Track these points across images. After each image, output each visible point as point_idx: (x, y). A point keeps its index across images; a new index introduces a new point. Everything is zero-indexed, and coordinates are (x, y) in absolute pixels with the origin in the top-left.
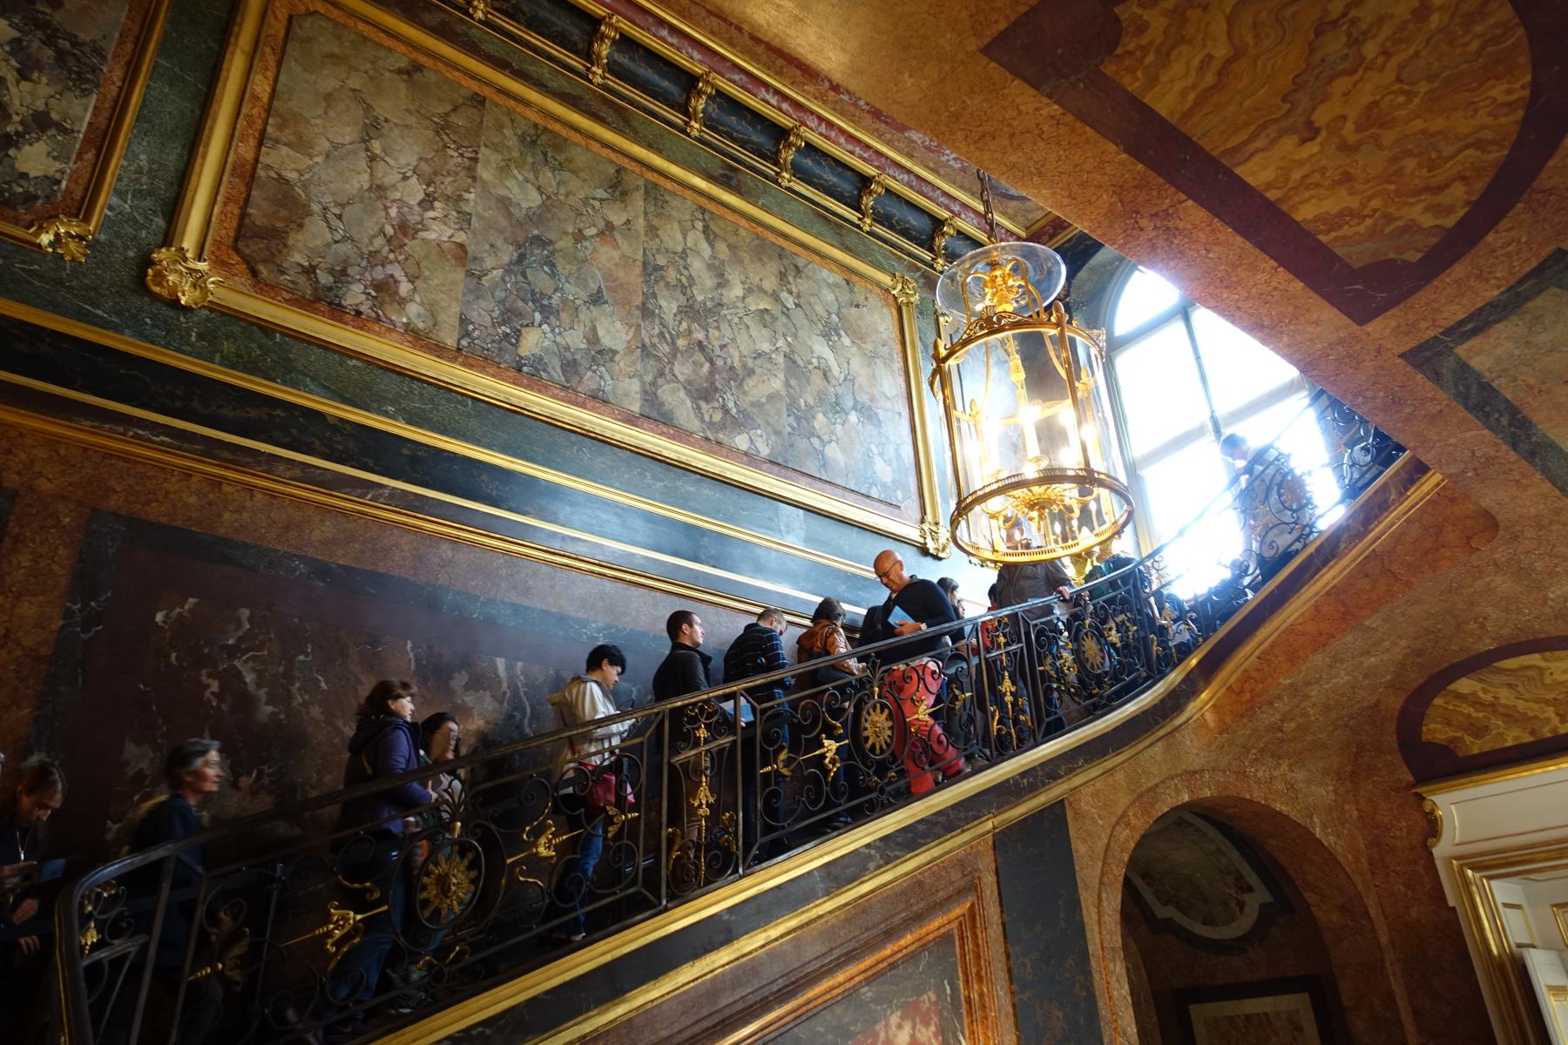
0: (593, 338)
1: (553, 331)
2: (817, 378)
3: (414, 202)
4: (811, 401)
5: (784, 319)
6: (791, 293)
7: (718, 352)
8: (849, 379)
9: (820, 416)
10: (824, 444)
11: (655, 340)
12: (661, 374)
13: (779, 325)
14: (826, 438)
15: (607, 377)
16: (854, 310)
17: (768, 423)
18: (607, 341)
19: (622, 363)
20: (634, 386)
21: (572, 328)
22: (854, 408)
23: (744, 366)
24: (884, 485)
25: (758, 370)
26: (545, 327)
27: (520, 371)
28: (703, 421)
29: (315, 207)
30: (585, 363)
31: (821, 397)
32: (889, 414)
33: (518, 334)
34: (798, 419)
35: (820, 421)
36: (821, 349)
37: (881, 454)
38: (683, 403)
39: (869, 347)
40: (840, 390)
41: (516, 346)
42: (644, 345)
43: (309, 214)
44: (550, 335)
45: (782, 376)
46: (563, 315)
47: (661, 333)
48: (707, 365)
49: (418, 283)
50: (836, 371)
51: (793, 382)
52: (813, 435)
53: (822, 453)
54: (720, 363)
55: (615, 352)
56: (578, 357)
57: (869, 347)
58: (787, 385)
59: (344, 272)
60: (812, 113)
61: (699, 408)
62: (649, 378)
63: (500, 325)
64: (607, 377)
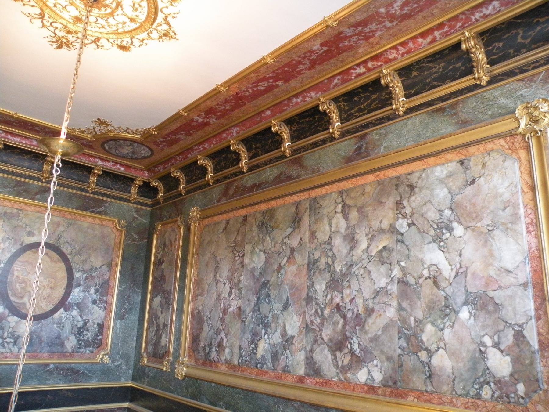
0: (284, 334)
1: (269, 337)
2: (427, 289)
3: (227, 296)
4: (420, 315)
5: (399, 247)
6: (405, 217)
7: (349, 306)
8: (461, 273)
9: (429, 328)
10: (430, 354)
11: (313, 317)
12: (315, 341)
13: (395, 256)
14: (433, 347)
15: (290, 356)
16: (469, 190)
17: (382, 352)
18: (290, 332)
19: (297, 344)
20: (301, 357)
21: (276, 331)
22: (465, 303)
23: (366, 309)
24: (498, 382)
25: (376, 308)
26: (266, 337)
27: (257, 367)
28: (337, 366)
29: (205, 318)
30: (280, 352)
31: (431, 307)
32: (509, 292)
33: (256, 345)
34: (408, 339)
35: (428, 334)
36: (434, 256)
37: (496, 345)
38: (327, 357)
39: (487, 221)
40: (449, 290)
41: (255, 354)
42: (307, 325)
43: (204, 323)
44: (268, 341)
45: (395, 304)
46: (273, 325)
47: (316, 310)
48: (342, 321)
49: (229, 337)
50: (447, 272)
51: (405, 305)
52: (421, 349)
53: (429, 365)
54: (349, 315)
55: (293, 337)
56: (278, 348)
57: (487, 221)
58: (400, 308)
59: (211, 344)
60: (386, 51)
61: (336, 357)
62: (308, 348)
63: (251, 344)
64: (290, 356)
